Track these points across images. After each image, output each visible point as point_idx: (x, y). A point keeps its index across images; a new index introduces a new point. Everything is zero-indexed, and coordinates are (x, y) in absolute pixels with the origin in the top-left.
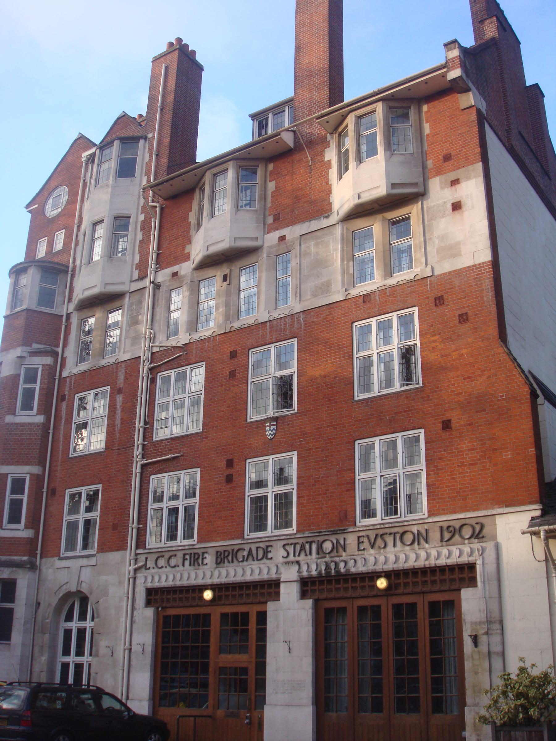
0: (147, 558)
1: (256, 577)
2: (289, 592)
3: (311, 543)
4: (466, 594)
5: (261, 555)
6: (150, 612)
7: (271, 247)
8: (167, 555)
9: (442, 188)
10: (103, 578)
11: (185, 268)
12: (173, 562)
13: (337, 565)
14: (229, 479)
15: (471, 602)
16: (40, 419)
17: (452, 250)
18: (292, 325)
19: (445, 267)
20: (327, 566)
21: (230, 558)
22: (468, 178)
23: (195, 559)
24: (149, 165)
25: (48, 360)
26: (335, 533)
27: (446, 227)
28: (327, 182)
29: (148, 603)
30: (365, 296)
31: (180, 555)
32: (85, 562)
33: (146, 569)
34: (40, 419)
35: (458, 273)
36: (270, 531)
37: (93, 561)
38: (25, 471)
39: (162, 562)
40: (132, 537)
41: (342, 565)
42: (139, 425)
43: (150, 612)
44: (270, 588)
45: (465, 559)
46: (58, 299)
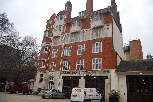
1: (78, 76)
2: (82, 78)
4: (106, 80)
5: (78, 73)
9: (106, 26)
11: (69, 33)
12: (66, 73)
13: (89, 75)
14: (74, 62)
15: (107, 81)
16: (48, 52)
17: (107, 34)
19: (106, 37)
20: (87, 75)
22: (110, 25)
23: (69, 73)
24: (64, 18)
25: (49, 44)
27: (106, 31)
32: (53, 72)
34: (48, 52)
35: (108, 38)
36: (80, 70)
38: (45, 59)
39: (64, 73)
40: (60, 69)
41: (90, 75)
42: (62, 54)
44: (80, 77)
45: (106, 75)
46: (51, 36)
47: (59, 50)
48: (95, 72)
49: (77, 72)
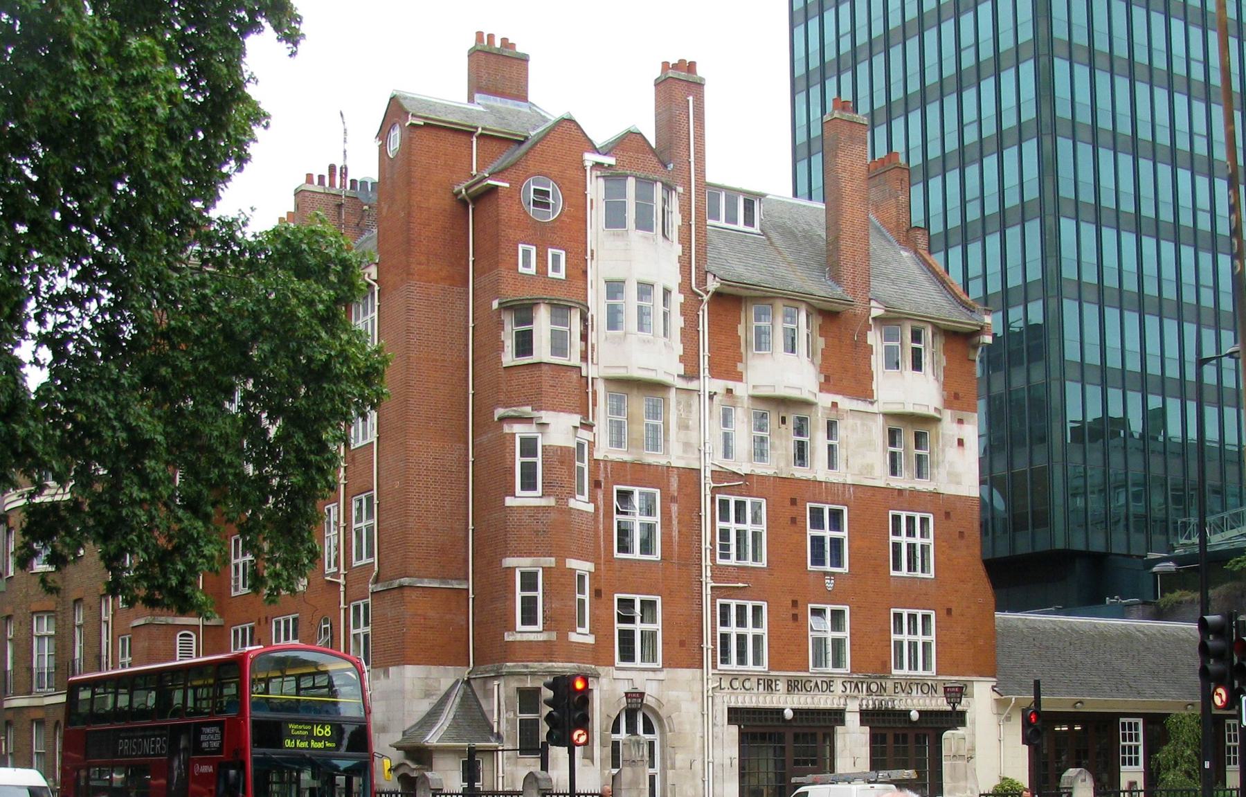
2: (852, 719)
6: (734, 729)
7: (824, 408)
11: (740, 389)
12: (747, 685)
17: (955, 478)
22: (969, 423)
23: (769, 685)
26: (881, 677)
29: (730, 721)
31: (754, 680)
32: (651, 675)
37: (661, 676)
39: (736, 684)
43: (734, 729)
44: (837, 716)
48: (908, 685)
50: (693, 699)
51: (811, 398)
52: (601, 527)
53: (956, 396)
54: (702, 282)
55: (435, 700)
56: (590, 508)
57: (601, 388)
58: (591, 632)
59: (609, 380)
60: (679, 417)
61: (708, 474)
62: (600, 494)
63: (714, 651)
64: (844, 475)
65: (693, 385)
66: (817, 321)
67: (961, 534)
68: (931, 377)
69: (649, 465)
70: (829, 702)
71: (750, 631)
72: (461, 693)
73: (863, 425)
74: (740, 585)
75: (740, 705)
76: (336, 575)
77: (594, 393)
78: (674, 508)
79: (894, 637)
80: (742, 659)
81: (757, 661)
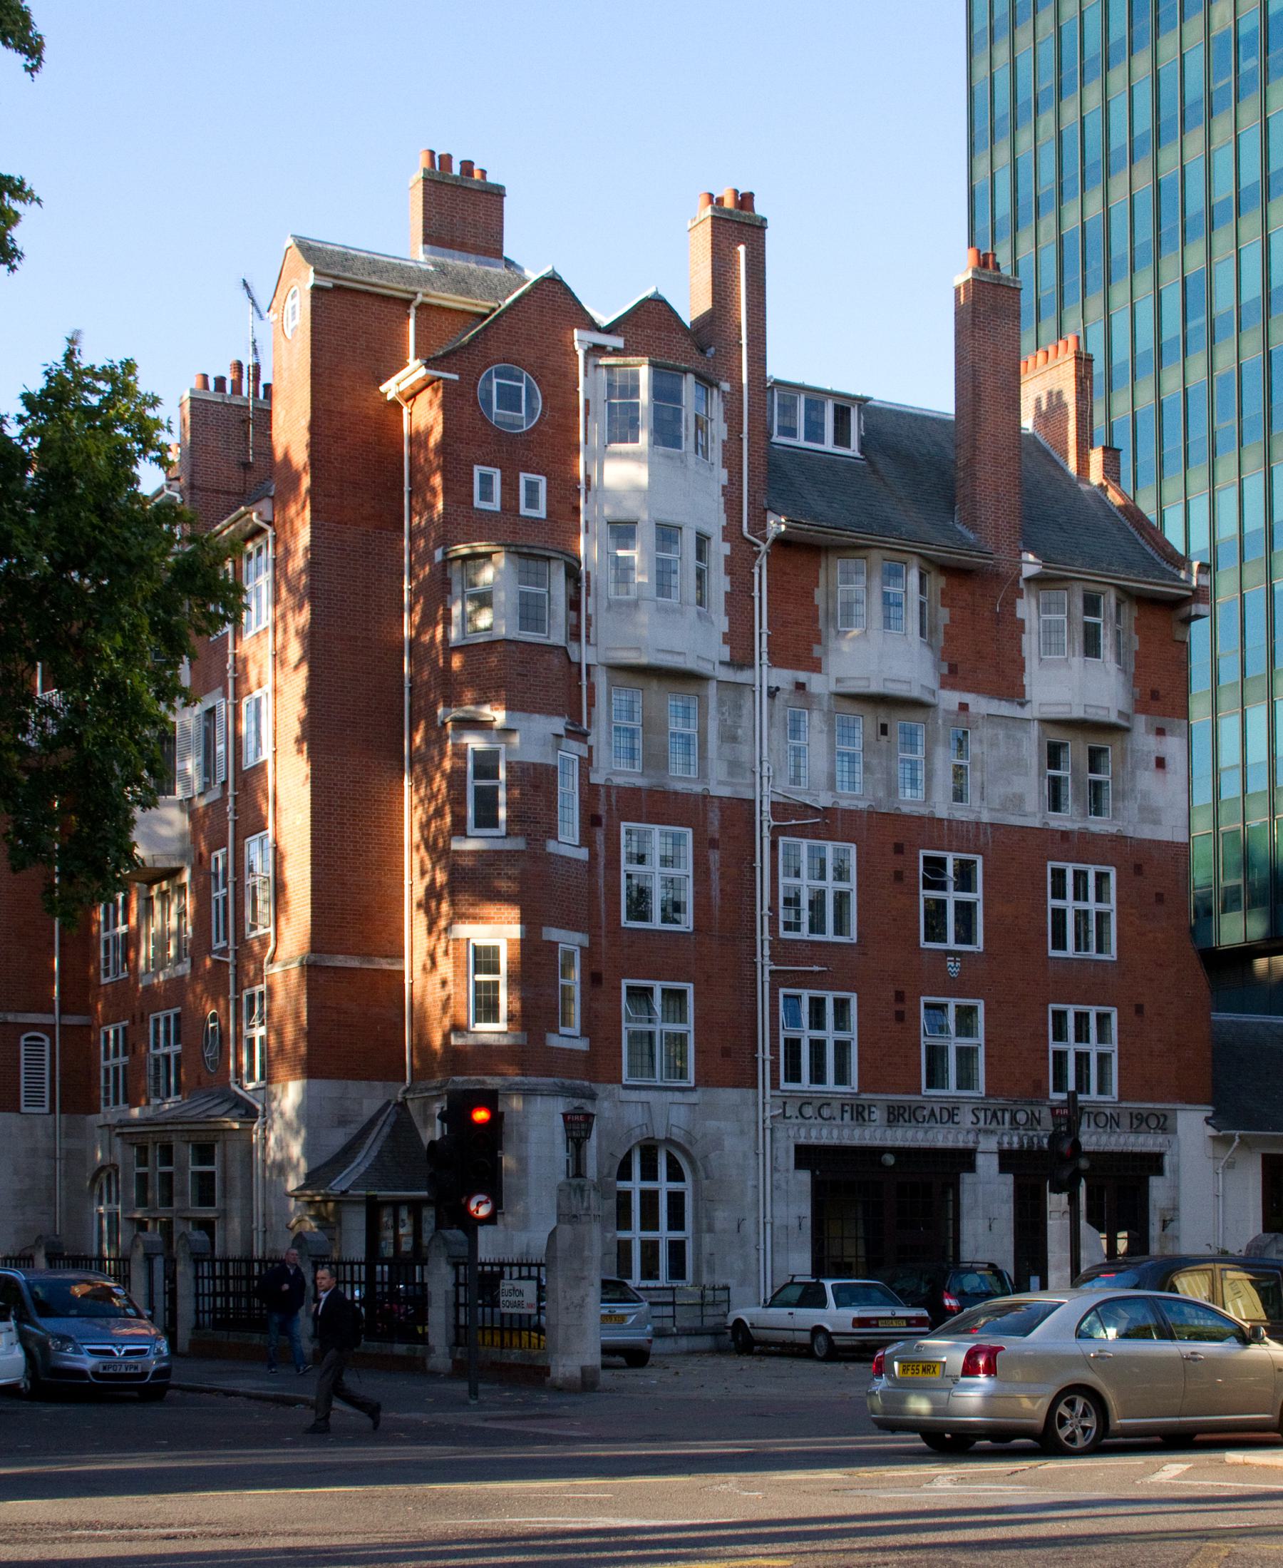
0: (785, 1103)
2: (987, 1164)
3: (1003, 1111)
4: (1154, 1181)
6: (805, 1176)
8: (817, 1103)
9: (1147, 732)
10: (712, 1124)
11: (818, 684)
12: (826, 1112)
14: (900, 1017)
15: (1158, 1189)
17: (1150, 814)
18: (977, 836)
20: (1031, 1139)
21: (906, 1116)
23: (859, 1113)
26: (1031, 1103)
28: (1020, 651)
29: (799, 1165)
30: (1063, 832)
31: (836, 1105)
32: (678, 1096)
33: (785, 1117)
35: (1157, 844)
36: (952, 1089)
39: (808, 1111)
43: (805, 1176)
44: (964, 1159)
45: (1156, 1149)
47: (714, 857)
49: (932, 1113)
50: (742, 1132)
51: (927, 698)
52: (601, 882)
53: (1155, 695)
54: (759, 524)
55: (353, 1129)
56: (583, 854)
57: (601, 679)
58: (584, 1034)
59: (618, 669)
60: (722, 722)
61: (767, 807)
62: (600, 835)
63: (775, 1065)
64: (977, 810)
65: (743, 677)
66: (937, 583)
67: (1160, 898)
68: (1112, 666)
69: (676, 793)
70: (951, 1137)
71: (830, 1035)
72: (392, 1119)
73: (1008, 736)
74: (816, 968)
75: (813, 1141)
76: (224, 952)
77: (591, 688)
78: (714, 857)
79: (1053, 1046)
80: (818, 1076)
81: (841, 1078)
